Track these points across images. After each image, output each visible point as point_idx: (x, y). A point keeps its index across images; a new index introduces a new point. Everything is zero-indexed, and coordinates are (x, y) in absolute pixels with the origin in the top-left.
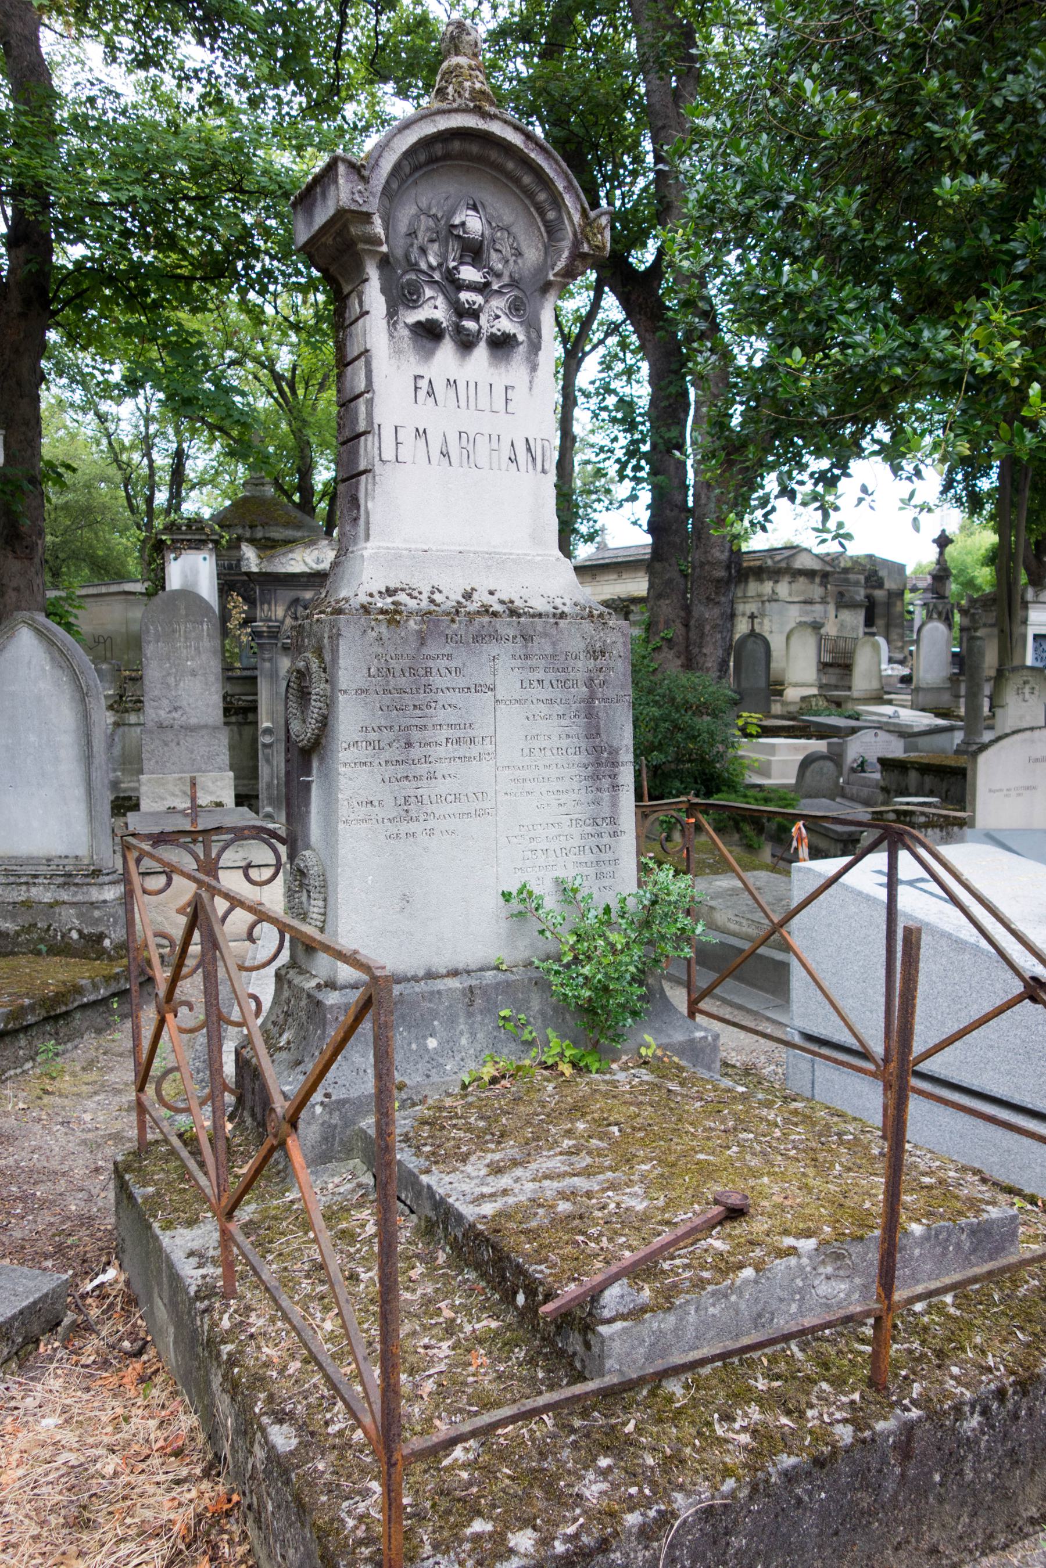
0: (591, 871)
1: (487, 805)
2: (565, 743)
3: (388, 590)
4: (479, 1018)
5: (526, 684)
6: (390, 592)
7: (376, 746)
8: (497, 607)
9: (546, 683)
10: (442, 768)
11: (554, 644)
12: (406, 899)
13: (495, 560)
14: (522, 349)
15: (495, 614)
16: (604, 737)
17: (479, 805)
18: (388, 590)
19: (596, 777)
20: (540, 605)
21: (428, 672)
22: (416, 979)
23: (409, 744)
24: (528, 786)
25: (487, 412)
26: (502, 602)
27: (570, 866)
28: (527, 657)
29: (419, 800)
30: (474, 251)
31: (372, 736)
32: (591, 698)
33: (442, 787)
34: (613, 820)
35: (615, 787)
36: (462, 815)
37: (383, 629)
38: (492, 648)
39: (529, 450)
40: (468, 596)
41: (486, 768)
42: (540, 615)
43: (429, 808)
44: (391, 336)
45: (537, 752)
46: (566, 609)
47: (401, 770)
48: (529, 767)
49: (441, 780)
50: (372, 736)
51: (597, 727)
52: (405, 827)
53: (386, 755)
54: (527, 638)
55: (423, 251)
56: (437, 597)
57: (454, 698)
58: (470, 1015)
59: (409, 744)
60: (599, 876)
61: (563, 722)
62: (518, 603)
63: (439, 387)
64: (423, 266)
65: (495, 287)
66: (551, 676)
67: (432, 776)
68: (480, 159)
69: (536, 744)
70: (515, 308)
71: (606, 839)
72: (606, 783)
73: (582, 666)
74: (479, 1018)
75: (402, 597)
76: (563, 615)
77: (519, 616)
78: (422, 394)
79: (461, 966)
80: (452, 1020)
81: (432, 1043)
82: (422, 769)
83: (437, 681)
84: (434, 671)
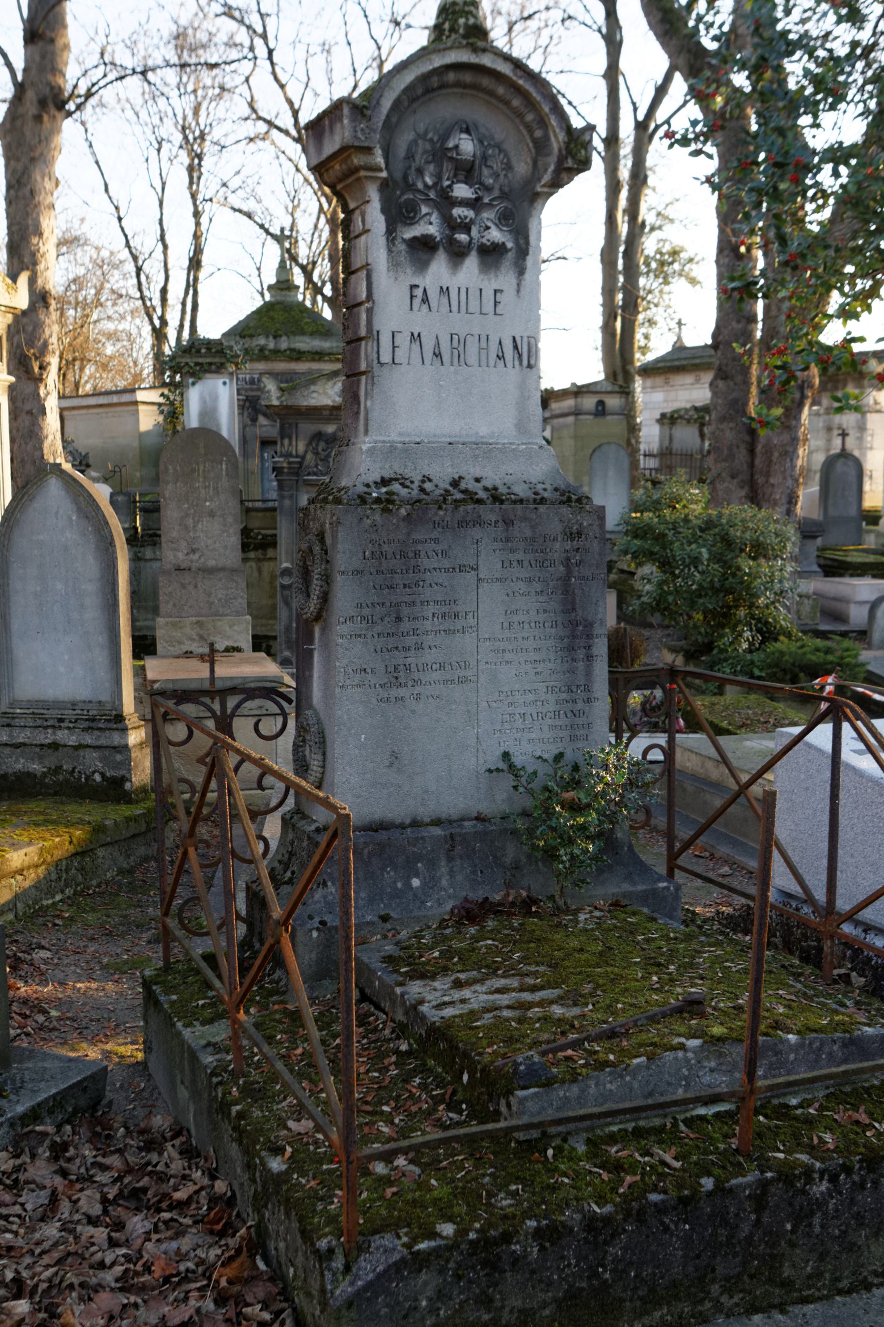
0: (565, 734)
1: (469, 673)
2: (542, 617)
3: (383, 479)
5: (506, 564)
6: (385, 482)
7: (370, 621)
8: (482, 495)
9: (526, 563)
10: (429, 640)
11: (533, 527)
12: (395, 756)
13: (482, 448)
14: (510, 255)
15: (480, 501)
16: (580, 612)
17: (462, 673)
18: (383, 479)
19: (571, 649)
20: (521, 491)
21: (417, 554)
22: (402, 826)
23: (399, 619)
24: (508, 656)
25: (477, 315)
26: (486, 489)
27: (545, 729)
28: (508, 540)
29: (408, 668)
30: (467, 171)
32: (566, 579)
33: (429, 656)
34: (587, 689)
35: (589, 658)
36: (446, 682)
37: (377, 517)
38: (477, 532)
39: (516, 347)
40: (455, 483)
41: (468, 641)
42: (521, 501)
43: (416, 676)
44: (390, 251)
45: (515, 625)
46: (546, 495)
47: (391, 642)
49: (427, 651)
50: (366, 612)
51: (573, 603)
52: (394, 692)
53: (378, 628)
54: (508, 523)
55: (420, 172)
56: (428, 486)
57: (442, 577)
58: (450, 859)
59: (399, 619)
60: (573, 738)
61: (541, 599)
62: (502, 490)
63: (433, 294)
64: (420, 186)
65: (486, 200)
66: (530, 556)
67: (419, 647)
68: (474, 87)
69: (515, 619)
70: (505, 219)
71: (580, 705)
72: (581, 654)
74: (458, 862)
75: (396, 487)
76: (543, 501)
77: (502, 502)
78: (417, 302)
79: (444, 816)
80: (432, 864)
81: (416, 882)
82: (411, 640)
83: (425, 563)
84: (423, 554)
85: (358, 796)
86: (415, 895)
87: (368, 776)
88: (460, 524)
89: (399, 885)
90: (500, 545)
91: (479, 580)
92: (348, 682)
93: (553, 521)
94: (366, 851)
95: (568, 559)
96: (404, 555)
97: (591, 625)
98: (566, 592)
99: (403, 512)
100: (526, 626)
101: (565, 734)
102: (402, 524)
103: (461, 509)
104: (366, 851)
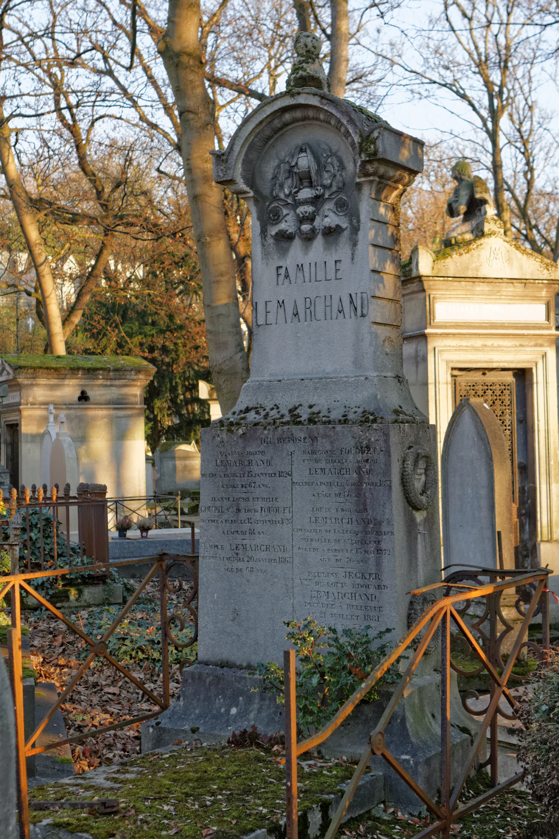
1: (286, 555)
2: (340, 514)
4: (267, 702)
5: (313, 471)
7: (220, 510)
9: (327, 471)
10: (258, 527)
11: (332, 443)
12: (236, 613)
13: (323, 382)
14: (346, 233)
16: (370, 512)
19: (363, 542)
21: (250, 462)
22: (240, 667)
23: (238, 510)
24: (315, 544)
25: (333, 281)
27: (345, 607)
28: (314, 452)
29: (244, 547)
30: (305, 179)
31: (218, 504)
32: (359, 483)
33: (259, 540)
36: (270, 560)
38: (290, 447)
39: (352, 302)
43: (250, 553)
44: (263, 245)
45: (320, 520)
47: (234, 527)
48: (315, 531)
49: (257, 535)
50: (218, 504)
51: (365, 504)
53: (225, 517)
57: (266, 480)
59: (238, 510)
61: (339, 500)
63: (292, 272)
64: (282, 196)
65: (326, 196)
66: (330, 466)
67: (252, 532)
70: (341, 206)
71: (372, 590)
72: (372, 547)
73: (352, 459)
74: (267, 702)
78: (282, 277)
80: (249, 699)
82: (246, 527)
83: (256, 469)
85: (213, 639)
86: (228, 720)
87: (219, 625)
88: (279, 440)
89: (223, 710)
90: (307, 456)
91: (293, 483)
92: (206, 554)
93: (347, 438)
94: (208, 680)
95: (360, 468)
96: (241, 463)
97: (380, 523)
98: (358, 495)
99: (240, 432)
100: (329, 521)
101: (361, 613)
102: (240, 441)
103: (280, 429)
104: (208, 680)
